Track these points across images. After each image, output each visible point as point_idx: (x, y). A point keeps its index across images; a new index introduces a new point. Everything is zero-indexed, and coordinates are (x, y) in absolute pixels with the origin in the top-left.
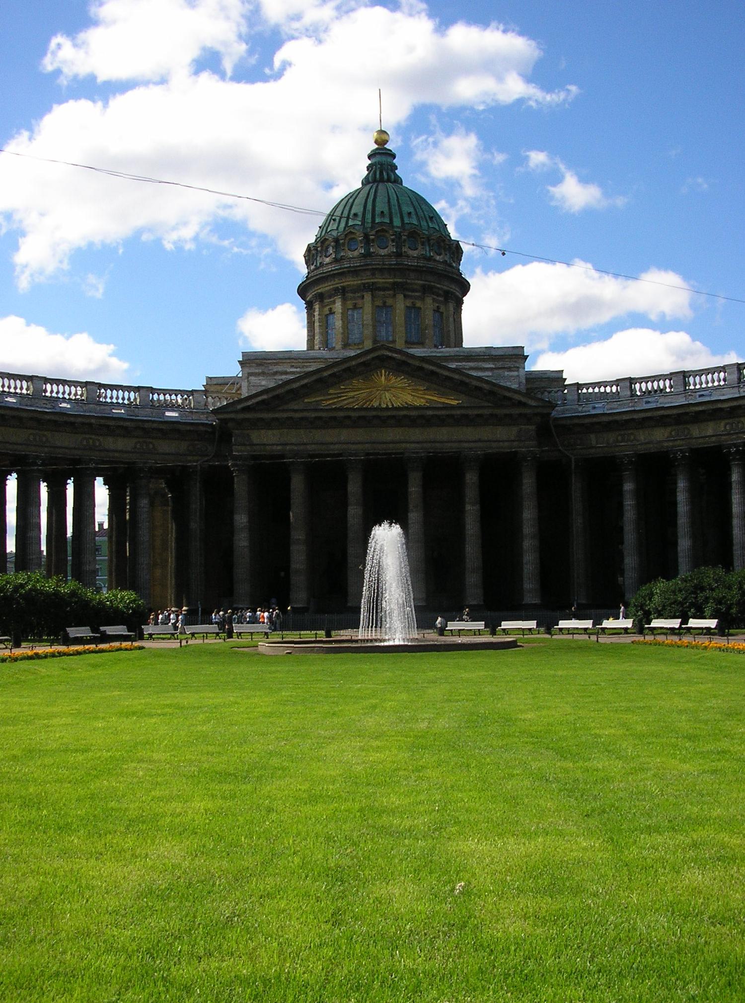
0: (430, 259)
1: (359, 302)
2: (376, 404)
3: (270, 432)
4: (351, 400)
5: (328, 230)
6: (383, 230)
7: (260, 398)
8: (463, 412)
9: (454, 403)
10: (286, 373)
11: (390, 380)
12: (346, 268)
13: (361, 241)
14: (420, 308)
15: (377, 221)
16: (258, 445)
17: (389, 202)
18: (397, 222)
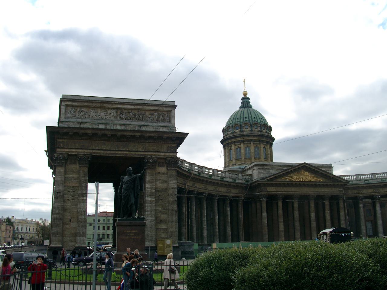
0: (268, 133)
1: (249, 145)
2: (301, 180)
3: (272, 188)
4: (295, 179)
5: (236, 121)
6: (256, 123)
7: (272, 177)
8: (327, 183)
9: (322, 180)
10: (269, 169)
11: (305, 173)
12: (246, 134)
13: (250, 126)
14: (266, 148)
15: (253, 120)
16: (269, 191)
17: (255, 114)
18: (259, 121)
